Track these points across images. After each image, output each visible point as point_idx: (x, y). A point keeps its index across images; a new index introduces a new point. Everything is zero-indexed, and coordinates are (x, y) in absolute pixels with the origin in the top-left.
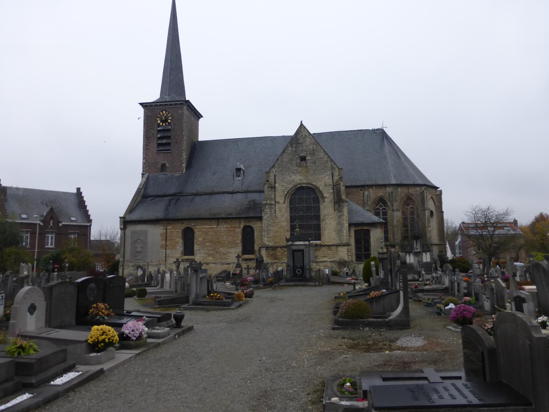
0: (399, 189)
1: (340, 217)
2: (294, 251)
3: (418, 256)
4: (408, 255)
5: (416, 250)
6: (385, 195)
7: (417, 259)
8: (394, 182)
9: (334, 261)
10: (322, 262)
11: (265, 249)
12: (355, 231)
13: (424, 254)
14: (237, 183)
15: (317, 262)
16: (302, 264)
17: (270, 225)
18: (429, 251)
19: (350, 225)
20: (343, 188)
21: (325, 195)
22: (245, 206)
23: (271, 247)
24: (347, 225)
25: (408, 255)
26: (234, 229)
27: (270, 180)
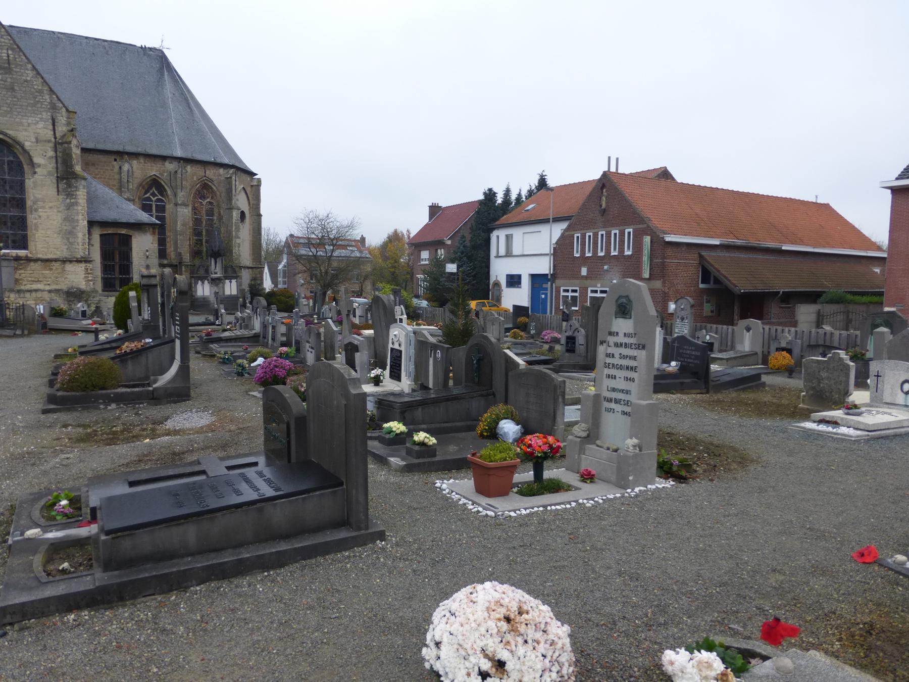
0: (189, 168)
1: (69, 207)
3: (217, 285)
4: (200, 282)
5: (214, 276)
6: (162, 175)
7: (216, 289)
8: (179, 153)
9: (57, 291)
10: (30, 291)
12: (101, 235)
13: (227, 281)
15: (19, 291)
18: (236, 277)
19: (91, 224)
20: (76, 152)
21: (36, 160)
24: (86, 223)
25: (200, 282)
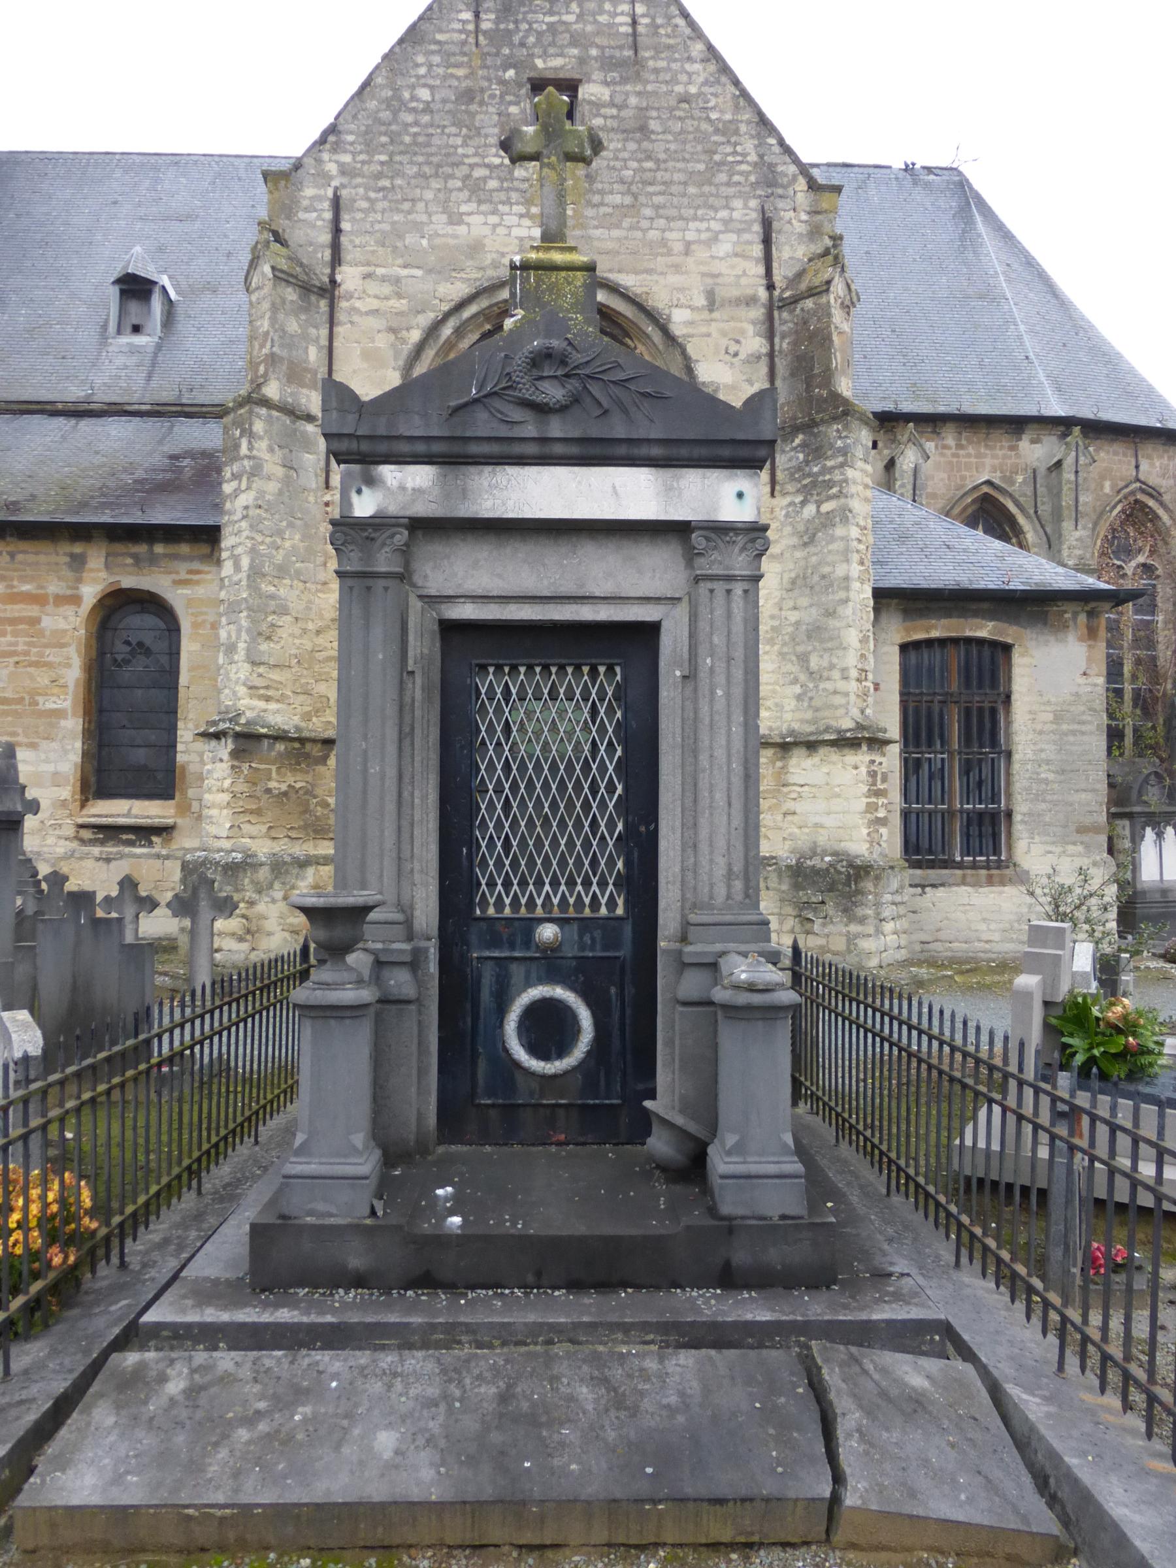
2: (476, 645)
4: (1149, 833)
6: (1012, 482)
8: (1056, 408)
11: (225, 749)
12: (904, 648)
14: (119, 365)
16: (611, 903)
17: (282, 571)
19: (883, 597)
22: (140, 474)
23: (280, 737)
25: (1149, 833)
26: (32, 611)
27: (296, 236)
